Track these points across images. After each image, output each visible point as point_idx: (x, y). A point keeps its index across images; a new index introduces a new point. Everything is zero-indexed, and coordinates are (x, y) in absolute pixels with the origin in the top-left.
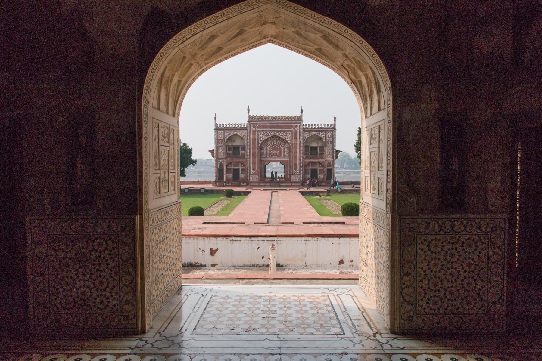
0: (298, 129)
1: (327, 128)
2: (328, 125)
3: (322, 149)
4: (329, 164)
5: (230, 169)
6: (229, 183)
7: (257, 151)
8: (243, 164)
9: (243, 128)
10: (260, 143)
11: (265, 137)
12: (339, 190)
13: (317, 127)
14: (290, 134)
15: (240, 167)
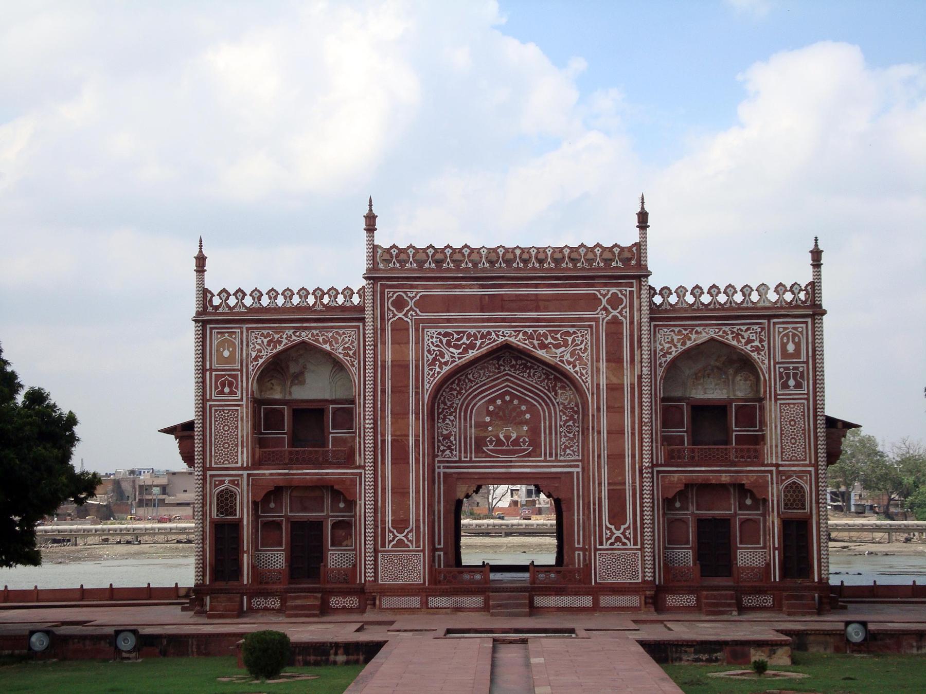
0: (622, 313)
1: (774, 306)
2: (780, 288)
3: (751, 413)
4: (795, 496)
5: (278, 525)
6: (266, 594)
7: (415, 427)
8: (342, 495)
9: (342, 308)
10: (429, 387)
11: (453, 357)
12: (855, 634)
13: (722, 298)
14: (584, 339)
15: (328, 515)
